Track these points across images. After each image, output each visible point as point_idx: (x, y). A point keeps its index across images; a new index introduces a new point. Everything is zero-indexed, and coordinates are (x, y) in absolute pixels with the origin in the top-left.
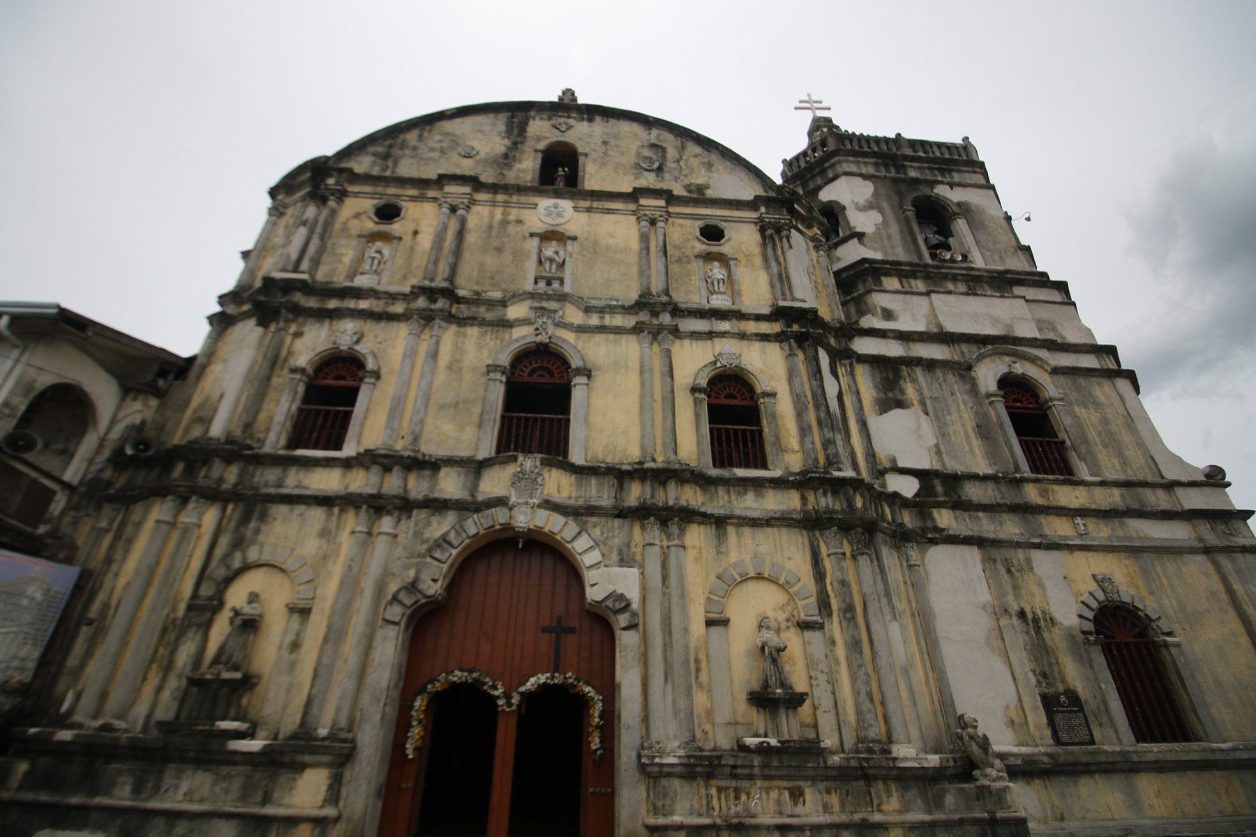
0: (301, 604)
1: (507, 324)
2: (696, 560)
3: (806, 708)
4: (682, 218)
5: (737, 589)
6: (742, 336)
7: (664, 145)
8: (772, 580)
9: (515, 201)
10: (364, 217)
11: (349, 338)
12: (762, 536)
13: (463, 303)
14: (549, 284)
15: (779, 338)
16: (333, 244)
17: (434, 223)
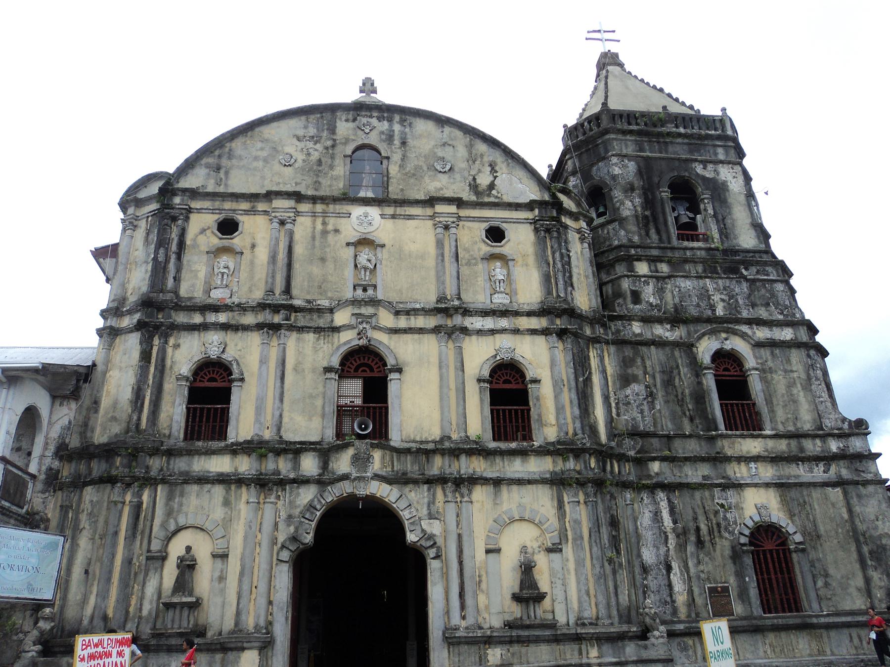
0: (220, 552)
1: (336, 330)
4: (470, 221)
5: (506, 529)
6: (516, 331)
7: (455, 145)
9: (332, 211)
10: (208, 232)
11: (216, 349)
12: (525, 491)
13: (300, 312)
14: (365, 290)
15: (545, 332)
16: (188, 261)
17: (268, 237)
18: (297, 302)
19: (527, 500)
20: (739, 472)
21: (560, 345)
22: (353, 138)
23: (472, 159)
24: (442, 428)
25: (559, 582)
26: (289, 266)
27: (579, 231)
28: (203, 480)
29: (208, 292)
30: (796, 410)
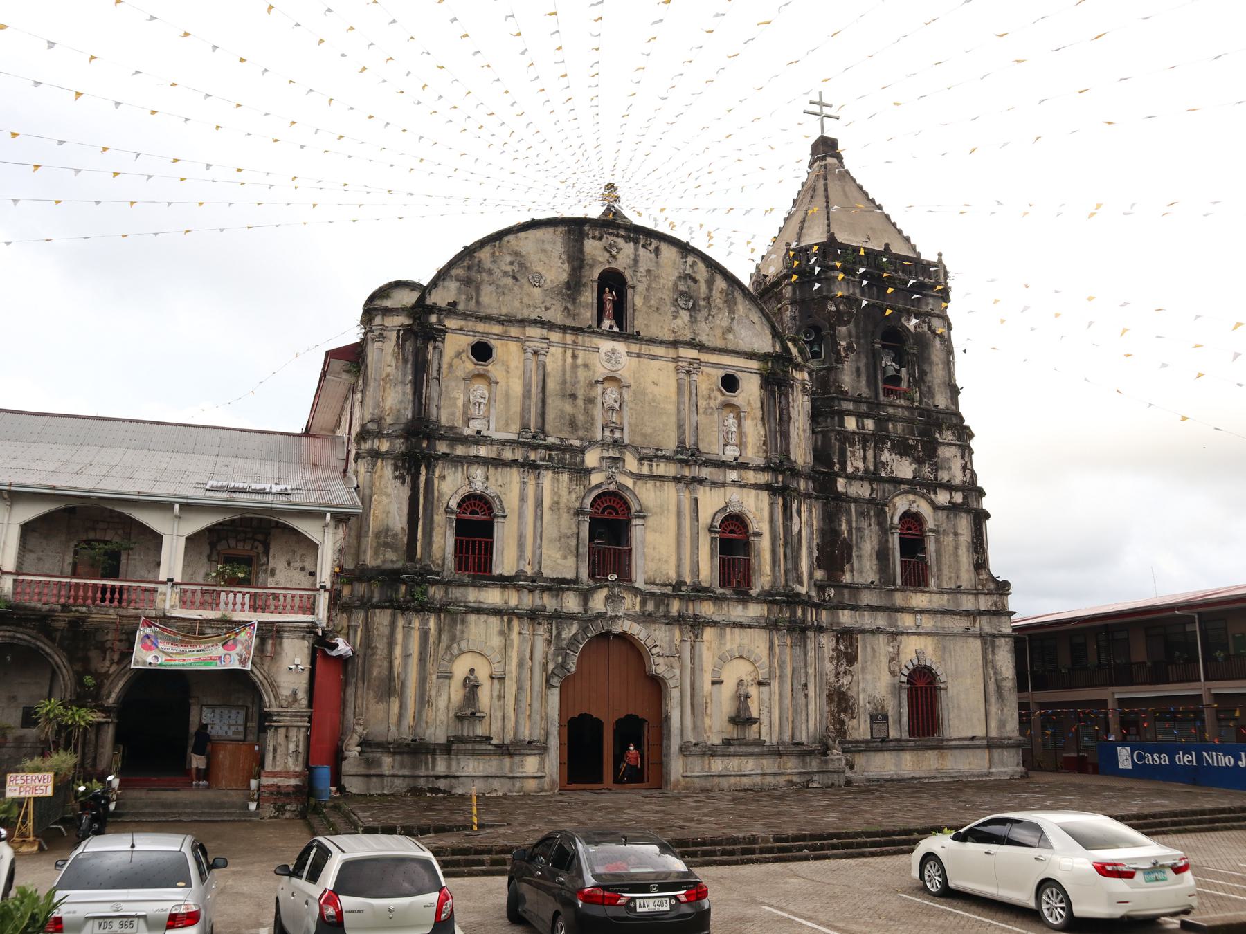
1: (588, 471)
3: (755, 727)
8: (747, 659)
14: (612, 431)
15: (767, 487)
18: (550, 440)
19: (746, 641)
20: (907, 621)
24: (679, 575)
25: (765, 710)
26: (544, 402)
29: (467, 423)
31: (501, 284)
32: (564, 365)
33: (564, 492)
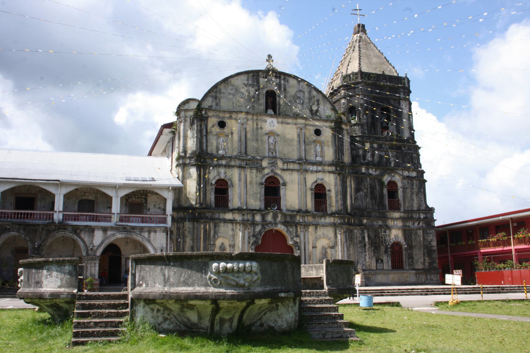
1: (263, 169)
2: (311, 235)
6: (324, 172)
10: (215, 127)
14: (272, 153)
16: (209, 139)
19: (325, 232)
21: (338, 178)
22: (266, 86)
23: (310, 99)
26: (246, 142)
27: (347, 130)
28: (225, 221)
29: (218, 151)
30: (413, 203)
31: (228, 98)
32: (253, 128)
33: (254, 176)
